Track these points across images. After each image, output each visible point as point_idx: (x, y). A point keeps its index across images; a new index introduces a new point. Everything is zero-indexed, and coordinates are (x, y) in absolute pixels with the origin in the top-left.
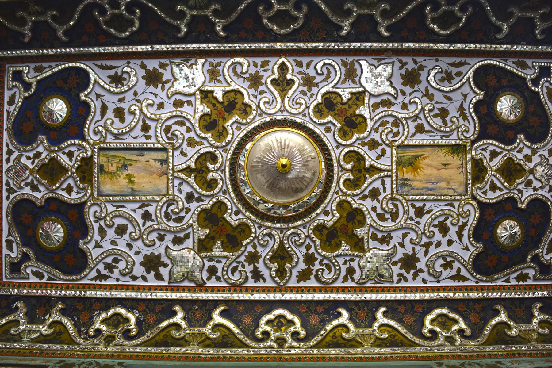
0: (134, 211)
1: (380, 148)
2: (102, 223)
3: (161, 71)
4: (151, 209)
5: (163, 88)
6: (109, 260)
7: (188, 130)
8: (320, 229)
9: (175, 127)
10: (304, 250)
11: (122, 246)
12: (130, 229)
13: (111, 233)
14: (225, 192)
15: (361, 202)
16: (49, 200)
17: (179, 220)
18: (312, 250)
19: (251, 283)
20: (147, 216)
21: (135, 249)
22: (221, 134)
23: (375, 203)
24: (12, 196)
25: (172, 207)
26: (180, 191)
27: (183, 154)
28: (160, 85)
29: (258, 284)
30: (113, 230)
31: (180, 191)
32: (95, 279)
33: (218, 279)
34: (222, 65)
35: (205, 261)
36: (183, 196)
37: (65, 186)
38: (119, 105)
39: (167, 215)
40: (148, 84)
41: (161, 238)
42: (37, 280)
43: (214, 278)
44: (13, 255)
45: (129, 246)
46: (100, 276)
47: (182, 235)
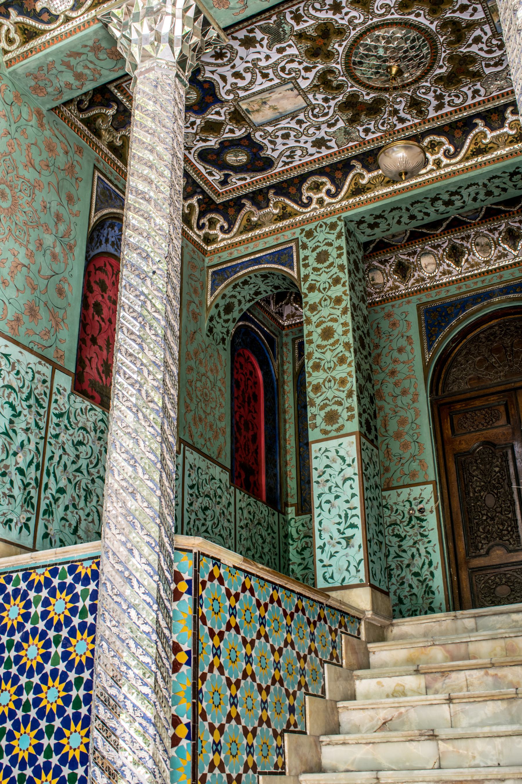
0: (289, 123)
1: (471, 8)
2: (269, 138)
3: (251, 35)
4: (301, 117)
5: (262, 46)
6: (288, 153)
7: (300, 63)
8: (440, 79)
9: (289, 66)
10: (432, 94)
11: (291, 143)
12: (292, 134)
13: (279, 141)
14: (352, 86)
15: (468, 50)
16: (221, 143)
17: (327, 114)
18: (439, 92)
19: (399, 126)
21: (302, 141)
22: (329, 55)
23: (480, 45)
24: (192, 151)
25: (317, 110)
26: (316, 99)
27: (305, 78)
28: (258, 45)
29: (405, 125)
30: (280, 138)
31: (316, 99)
32: (284, 166)
33: (373, 133)
34: (301, 9)
35: (358, 128)
36: (320, 102)
37: (227, 130)
38: (234, 71)
39: (314, 116)
40: (247, 48)
41: (319, 129)
42: (243, 182)
43: (370, 134)
44: (217, 177)
45: (296, 141)
46: (286, 164)
47: (333, 121)
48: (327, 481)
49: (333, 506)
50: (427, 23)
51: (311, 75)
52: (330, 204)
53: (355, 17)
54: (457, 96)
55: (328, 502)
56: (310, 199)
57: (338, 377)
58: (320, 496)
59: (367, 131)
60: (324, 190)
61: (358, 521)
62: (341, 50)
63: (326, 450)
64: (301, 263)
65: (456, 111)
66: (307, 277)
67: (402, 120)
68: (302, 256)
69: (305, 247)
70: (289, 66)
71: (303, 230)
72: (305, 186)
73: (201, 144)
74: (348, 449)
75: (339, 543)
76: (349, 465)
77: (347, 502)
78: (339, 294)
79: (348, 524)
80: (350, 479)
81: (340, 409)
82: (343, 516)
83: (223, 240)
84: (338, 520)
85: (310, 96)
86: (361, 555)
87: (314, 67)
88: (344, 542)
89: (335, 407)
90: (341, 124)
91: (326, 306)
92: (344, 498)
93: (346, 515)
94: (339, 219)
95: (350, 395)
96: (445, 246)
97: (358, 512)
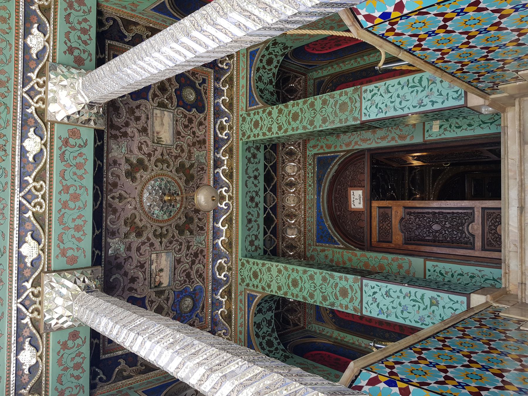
48: (387, 308)
55: (402, 312)
58: (397, 317)
63: (367, 303)
64: (255, 289)
66: (263, 289)
68: (252, 288)
69: (248, 285)
71: (240, 284)
76: (380, 289)
79: (420, 301)
82: (414, 303)
88: (434, 308)
94: (241, 260)
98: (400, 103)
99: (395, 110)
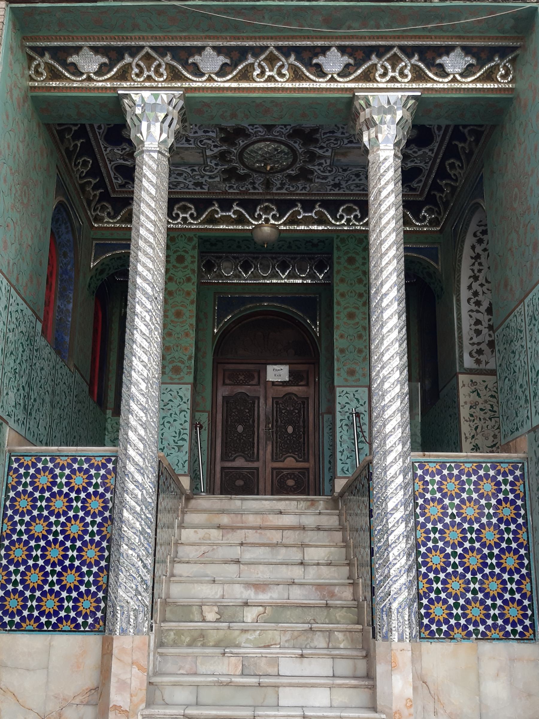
4: (196, 168)
7: (213, 142)
8: (289, 176)
9: (205, 141)
11: (181, 179)
12: (185, 175)
19: (252, 191)
20: (193, 170)
26: (211, 162)
36: (213, 165)
48: (170, 409)
49: (172, 425)
50: (298, 148)
51: (216, 150)
52: (191, 223)
53: (260, 132)
54: (293, 187)
56: (178, 215)
57: (183, 345)
59: (230, 187)
60: (189, 213)
61: (187, 437)
62: (242, 144)
63: (171, 390)
65: (288, 194)
67: (254, 188)
70: (205, 141)
72: (177, 206)
73: (122, 161)
74: (185, 392)
75: (173, 448)
76: (185, 403)
77: (181, 424)
78: (189, 289)
80: (185, 411)
81: (182, 366)
82: (178, 432)
83: (108, 222)
84: (174, 434)
85: (208, 160)
86: (187, 457)
87: (220, 147)
88: (176, 448)
89: (179, 364)
90: (217, 179)
91: (180, 295)
92: (179, 422)
93: (180, 432)
94: (195, 235)
95: (190, 358)
96: (241, 259)
97: (188, 432)
98: (346, 425)
99: (341, 420)
